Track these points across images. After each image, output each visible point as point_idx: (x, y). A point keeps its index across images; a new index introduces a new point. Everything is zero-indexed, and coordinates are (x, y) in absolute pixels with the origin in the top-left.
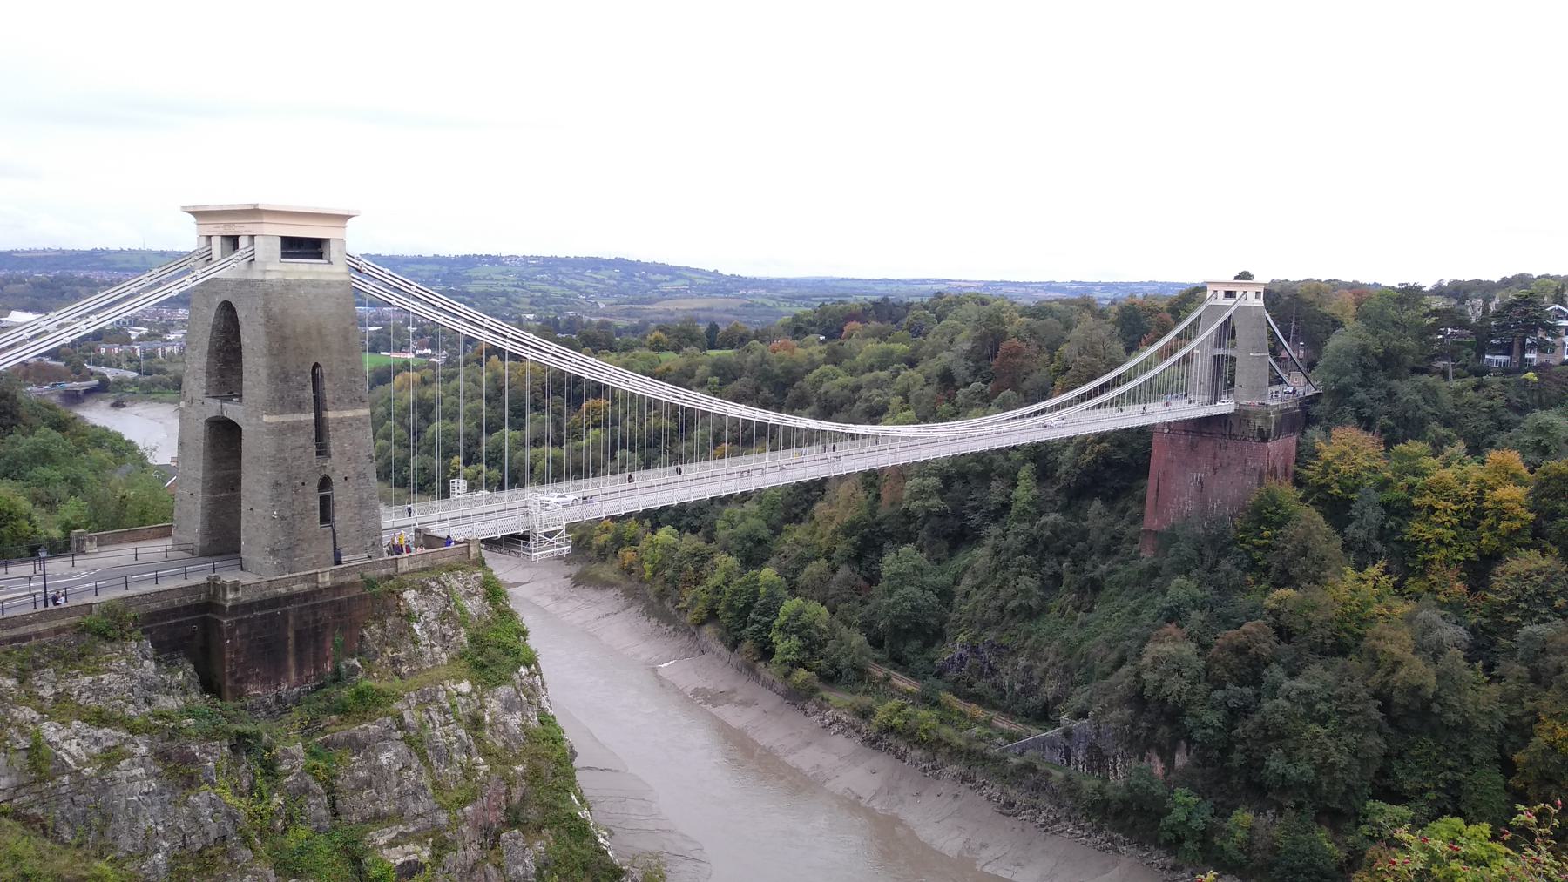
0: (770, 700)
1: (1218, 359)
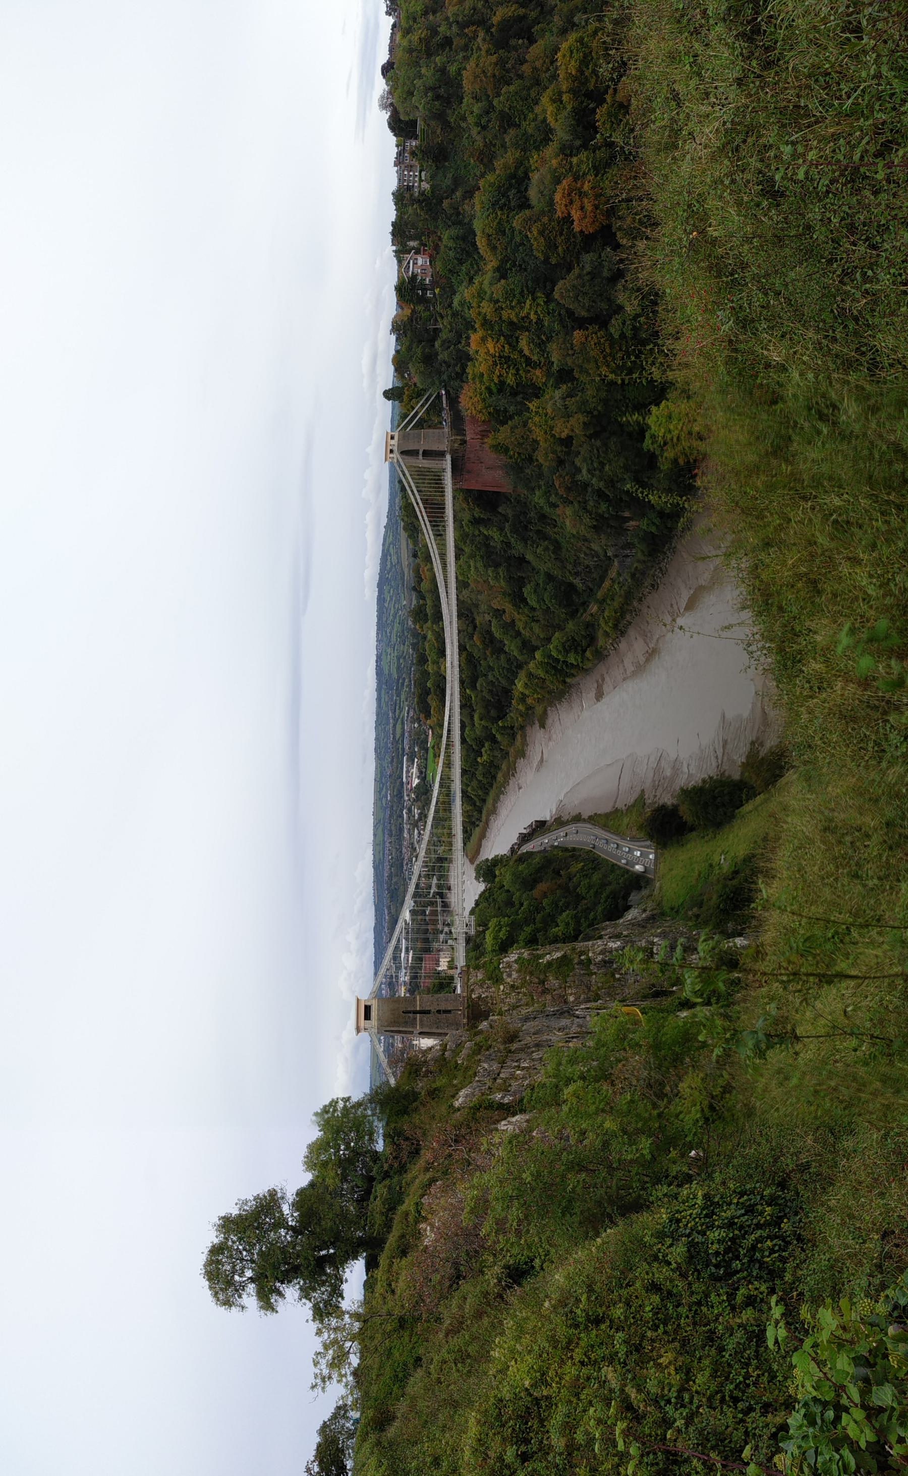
0: (601, 668)
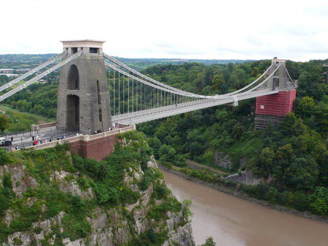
1: (274, 79)
